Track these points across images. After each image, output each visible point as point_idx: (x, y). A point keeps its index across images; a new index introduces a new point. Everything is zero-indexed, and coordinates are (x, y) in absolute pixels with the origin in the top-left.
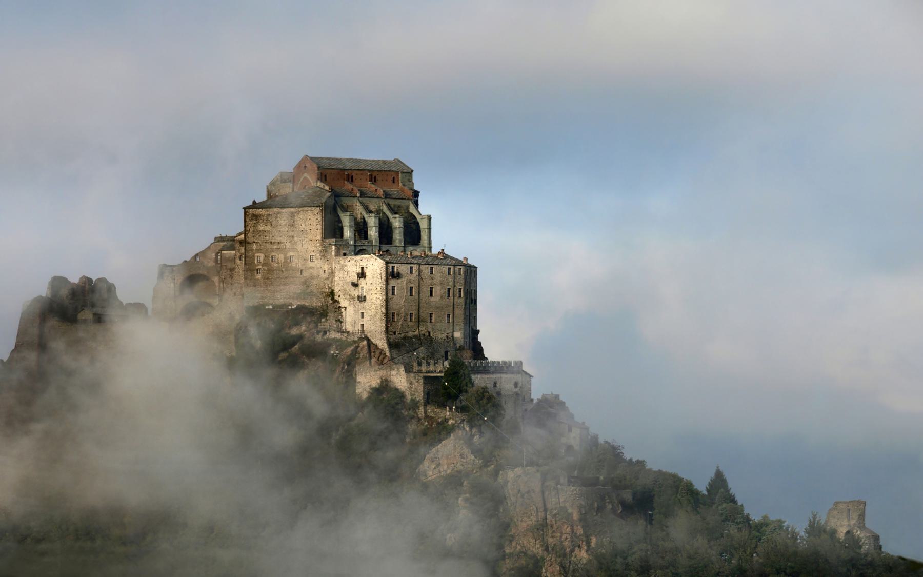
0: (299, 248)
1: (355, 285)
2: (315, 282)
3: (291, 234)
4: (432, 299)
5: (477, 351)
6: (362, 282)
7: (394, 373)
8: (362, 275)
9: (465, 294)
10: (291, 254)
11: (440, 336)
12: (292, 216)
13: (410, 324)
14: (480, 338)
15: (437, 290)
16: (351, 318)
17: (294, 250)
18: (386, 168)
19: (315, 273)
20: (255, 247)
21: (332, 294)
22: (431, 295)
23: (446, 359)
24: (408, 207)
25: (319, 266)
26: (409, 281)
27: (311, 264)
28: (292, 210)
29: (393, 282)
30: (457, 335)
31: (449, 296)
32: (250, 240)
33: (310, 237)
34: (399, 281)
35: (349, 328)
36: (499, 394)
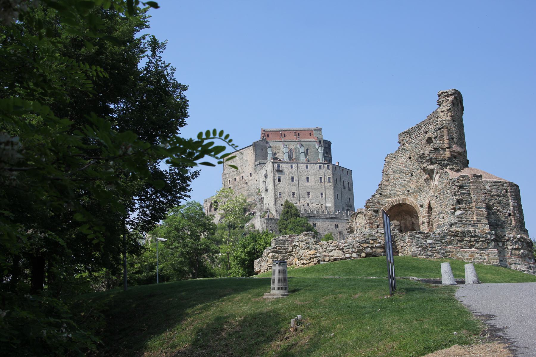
0: (245, 171)
2: (252, 188)
3: (241, 164)
4: (308, 184)
9: (334, 180)
10: (242, 175)
13: (294, 199)
17: (242, 172)
20: (227, 176)
22: (308, 181)
27: (251, 178)
30: (329, 205)
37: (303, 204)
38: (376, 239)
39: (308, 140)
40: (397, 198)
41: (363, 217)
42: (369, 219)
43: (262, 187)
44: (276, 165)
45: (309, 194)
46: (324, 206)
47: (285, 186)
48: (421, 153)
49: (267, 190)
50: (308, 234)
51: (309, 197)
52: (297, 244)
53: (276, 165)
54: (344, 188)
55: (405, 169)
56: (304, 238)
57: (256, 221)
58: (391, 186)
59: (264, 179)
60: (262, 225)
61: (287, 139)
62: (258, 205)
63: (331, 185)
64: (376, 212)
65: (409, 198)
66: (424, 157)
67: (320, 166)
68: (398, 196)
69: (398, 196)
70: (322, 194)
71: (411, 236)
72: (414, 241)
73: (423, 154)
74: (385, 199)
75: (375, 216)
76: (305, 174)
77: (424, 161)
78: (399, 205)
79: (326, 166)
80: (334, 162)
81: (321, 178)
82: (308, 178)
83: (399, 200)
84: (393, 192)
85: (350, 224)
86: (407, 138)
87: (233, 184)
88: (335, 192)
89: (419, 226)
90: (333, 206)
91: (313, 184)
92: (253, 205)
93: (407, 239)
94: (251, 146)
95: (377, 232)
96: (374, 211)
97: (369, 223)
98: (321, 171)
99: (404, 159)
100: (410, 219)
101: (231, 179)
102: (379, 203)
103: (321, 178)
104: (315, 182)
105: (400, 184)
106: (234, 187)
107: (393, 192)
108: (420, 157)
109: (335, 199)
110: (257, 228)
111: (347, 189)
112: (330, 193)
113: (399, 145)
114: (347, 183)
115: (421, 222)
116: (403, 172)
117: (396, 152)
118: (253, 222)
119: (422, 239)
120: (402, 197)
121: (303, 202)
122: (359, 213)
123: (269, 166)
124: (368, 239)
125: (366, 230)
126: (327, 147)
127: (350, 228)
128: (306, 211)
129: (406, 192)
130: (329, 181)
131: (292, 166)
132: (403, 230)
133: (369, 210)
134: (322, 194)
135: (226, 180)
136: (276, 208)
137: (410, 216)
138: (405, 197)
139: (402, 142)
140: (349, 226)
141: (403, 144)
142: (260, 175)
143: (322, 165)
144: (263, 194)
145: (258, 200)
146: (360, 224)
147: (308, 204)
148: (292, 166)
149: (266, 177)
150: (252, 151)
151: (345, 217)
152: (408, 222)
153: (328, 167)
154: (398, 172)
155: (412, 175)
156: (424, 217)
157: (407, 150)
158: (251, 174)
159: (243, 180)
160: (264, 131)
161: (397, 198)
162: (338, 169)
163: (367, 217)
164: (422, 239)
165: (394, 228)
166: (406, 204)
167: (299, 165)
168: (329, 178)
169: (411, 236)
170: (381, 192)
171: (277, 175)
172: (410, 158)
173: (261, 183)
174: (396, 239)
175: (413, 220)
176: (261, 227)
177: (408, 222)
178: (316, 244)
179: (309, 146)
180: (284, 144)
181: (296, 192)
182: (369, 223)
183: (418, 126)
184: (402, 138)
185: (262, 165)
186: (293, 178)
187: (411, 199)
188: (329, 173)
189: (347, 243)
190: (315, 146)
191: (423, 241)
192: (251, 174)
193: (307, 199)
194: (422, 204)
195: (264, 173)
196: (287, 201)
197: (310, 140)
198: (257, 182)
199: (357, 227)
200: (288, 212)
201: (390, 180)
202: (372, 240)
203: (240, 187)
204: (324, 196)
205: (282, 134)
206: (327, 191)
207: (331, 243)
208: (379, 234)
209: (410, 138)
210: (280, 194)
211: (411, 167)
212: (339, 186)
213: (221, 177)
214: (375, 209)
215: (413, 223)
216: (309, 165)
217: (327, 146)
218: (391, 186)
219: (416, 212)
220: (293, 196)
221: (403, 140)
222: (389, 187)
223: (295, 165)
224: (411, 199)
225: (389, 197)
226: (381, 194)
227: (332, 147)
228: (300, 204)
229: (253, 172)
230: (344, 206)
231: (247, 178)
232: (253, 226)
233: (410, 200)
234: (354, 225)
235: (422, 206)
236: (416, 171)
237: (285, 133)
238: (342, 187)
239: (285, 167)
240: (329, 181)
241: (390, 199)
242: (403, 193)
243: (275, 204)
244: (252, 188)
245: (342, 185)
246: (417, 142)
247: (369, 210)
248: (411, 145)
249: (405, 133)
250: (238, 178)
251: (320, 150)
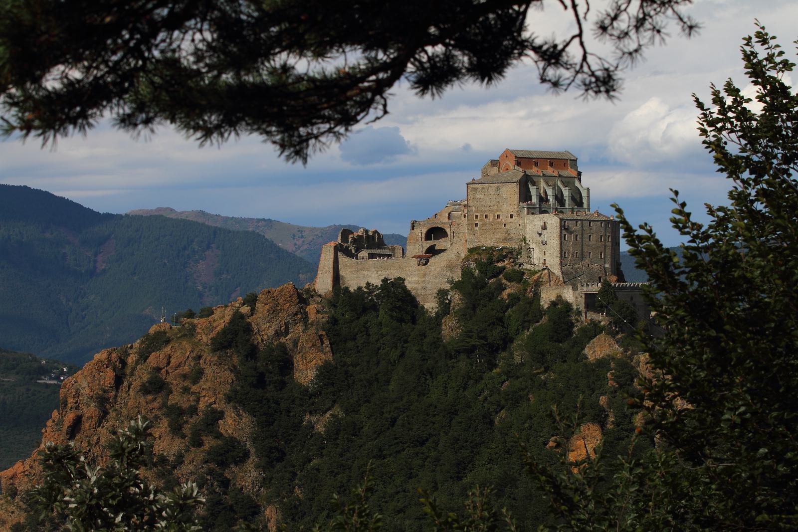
1: (540, 234)
2: (513, 232)
4: (590, 243)
5: (621, 278)
6: (544, 232)
7: (565, 291)
8: (544, 228)
12: (498, 188)
14: (622, 268)
16: (537, 255)
18: (559, 157)
19: (513, 226)
20: (474, 209)
21: (525, 239)
23: (600, 282)
24: (574, 183)
27: (511, 220)
29: (564, 232)
32: (470, 204)
34: (684, 39)
35: (536, 262)
36: (634, 305)
91: (594, 242)
158: (511, 216)
229: (515, 214)
250: (491, 216)
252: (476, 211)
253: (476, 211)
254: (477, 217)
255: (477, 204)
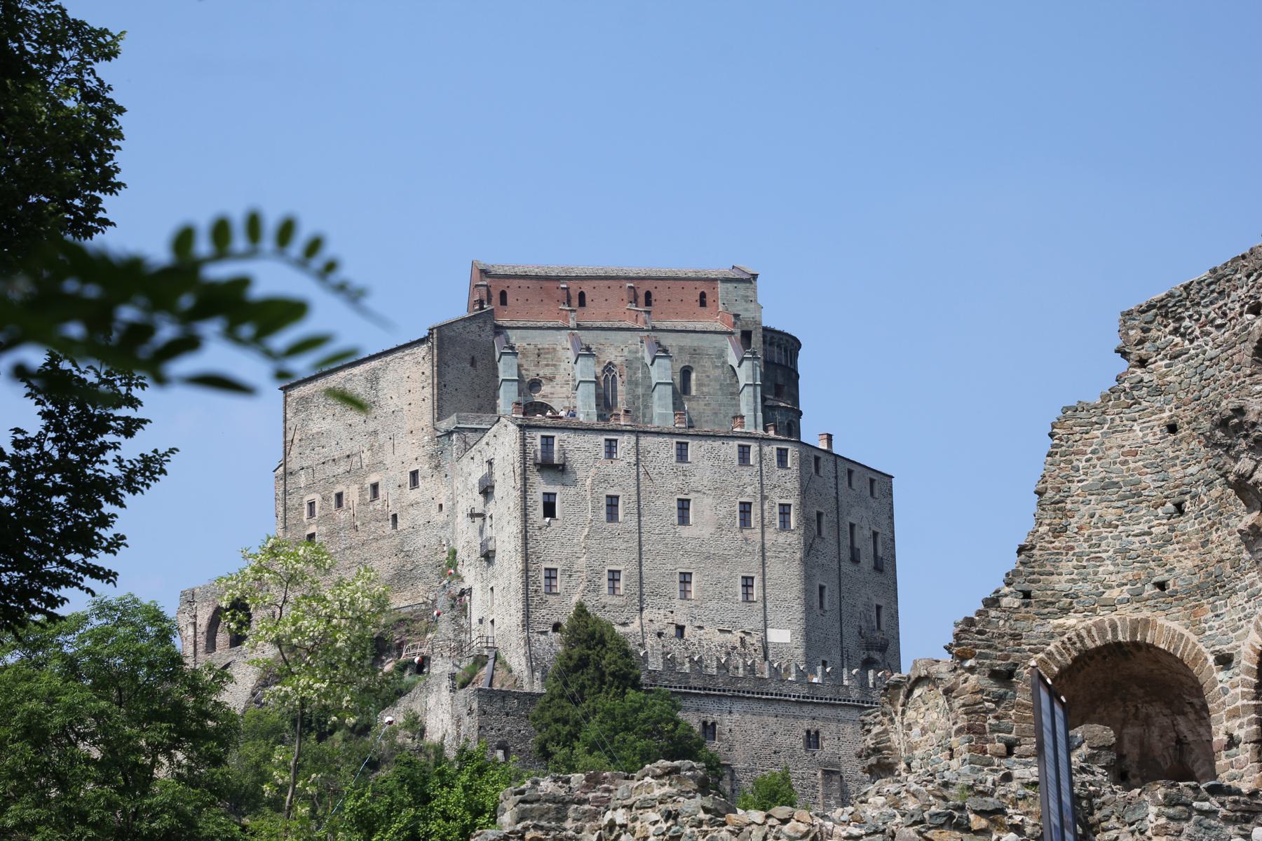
0: (389, 459)
2: (420, 541)
4: (685, 531)
9: (805, 519)
10: (373, 478)
11: (720, 638)
13: (616, 600)
15: (701, 508)
17: (374, 467)
20: (302, 480)
22: (684, 519)
25: (428, 495)
26: (606, 480)
27: (413, 495)
28: (374, 364)
30: (780, 636)
31: (745, 522)
33: (407, 427)
37: (656, 627)
38: (1001, 811)
39: (690, 326)
40: (1106, 616)
41: (942, 701)
42: (970, 709)
43: (465, 537)
44: (536, 438)
45: (685, 578)
46: (753, 640)
47: (574, 539)
48: (1227, 405)
49: (488, 556)
50: (676, 770)
51: (685, 594)
52: (620, 817)
53: (536, 438)
54: (855, 559)
55: (1147, 479)
56: (657, 793)
57: (432, 701)
58: (1079, 556)
59: (478, 503)
60: (458, 722)
61: (594, 314)
62: (445, 628)
63: (790, 541)
64: (1004, 677)
65: (1161, 620)
66: (1240, 426)
67: (744, 453)
68: (1112, 606)
69: (1112, 606)
70: (747, 583)
71: (1170, 802)
72: (1188, 827)
73: (1240, 411)
74: (1045, 617)
75: (999, 700)
76: (673, 483)
77: (1243, 444)
78: (1115, 649)
79: (771, 450)
80: (810, 432)
81: (745, 508)
82: (684, 506)
83: (1114, 627)
84: (1087, 587)
85: (876, 729)
86: (1162, 334)
87: (327, 518)
88: (808, 578)
89: (1210, 759)
90: (799, 641)
92: (421, 625)
93: (1152, 815)
94: (421, 341)
95: (1007, 778)
96: (995, 675)
97: (970, 729)
98: (748, 476)
99: (1143, 432)
100: (1166, 721)
101: (317, 498)
102: (1016, 637)
103: (745, 508)
104: (720, 527)
105: (1123, 551)
106: (332, 534)
107: (1087, 587)
108: (1223, 424)
109: (808, 609)
110: (433, 736)
111: (867, 562)
112: (785, 577)
113: (1123, 365)
114: (868, 533)
115: (1219, 737)
116: (1137, 494)
117: (1105, 398)
118: (416, 707)
119: (1226, 819)
120: (1128, 613)
121: (657, 617)
122: (919, 681)
123: (503, 444)
124: (961, 808)
125: (955, 763)
126: (779, 359)
127: (876, 750)
128: (670, 662)
129: (1149, 590)
130: (785, 524)
131: (611, 447)
132: (1133, 770)
133: (971, 670)
134: (747, 583)
135: (293, 501)
136: (528, 642)
137: (1169, 704)
138: (1146, 613)
139: (1136, 352)
140: (870, 742)
141: (1142, 363)
142: (458, 483)
143: (754, 448)
144: (470, 575)
145: (443, 602)
146: (924, 731)
147: (680, 629)
148: (611, 447)
149: (487, 491)
150: (427, 368)
151: (855, 695)
152: (1156, 732)
153: (782, 454)
154: (1112, 494)
155: (1179, 508)
156: (1234, 714)
157: (1158, 391)
158: (414, 474)
159: (378, 504)
160: (485, 273)
161: (1106, 616)
162: (827, 466)
163: (957, 703)
164: (1226, 819)
165: (1090, 758)
166: (1150, 647)
167: (646, 441)
168: (785, 510)
169: (1170, 802)
170: (1026, 586)
171: (540, 486)
172: (1172, 429)
173: (462, 521)
174: (1098, 815)
175: (1183, 726)
176: (451, 730)
177: (1156, 732)
178: (712, 823)
179: (695, 352)
180: (576, 342)
181: (626, 569)
182: (970, 729)
183: (1217, 276)
184: (1135, 334)
185: (468, 435)
186: (612, 502)
187: (1174, 625)
188: (786, 486)
189: (861, 822)
190: (721, 354)
191: (1231, 830)
192: (414, 474)
193: (677, 603)
194: (1225, 648)
195: (479, 472)
196: (581, 610)
197: (699, 326)
198: (442, 518)
199: (912, 748)
200: (583, 663)
201: (1073, 528)
202: (981, 813)
203: (362, 536)
204: (756, 592)
205: (570, 292)
206: (775, 569)
207: (784, 822)
208: (1014, 785)
209: (1175, 331)
210: (551, 574)
211: (1176, 473)
212: (828, 547)
213: (269, 487)
214: (1000, 665)
215: (1180, 741)
216: (693, 445)
217: (777, 355)
218: (1079, 556)
219: (1198, 690)
220: (613, 590)
221: (1141, 342)
222: (1067, 565)
223: (625, 443)
224: (1174, 625)
225: (1065, 611)
226: (1027, 595)
227: (805, 363)
228: (641, 629)
229: (424, 468)
230: (852, 642)
231: (394, 493)
232: (416, 726)
233: (1168, 628)
234: (896, 739)
235: (1225, 661)
236: (1201, 489)
237: (586, 287)
238: (846, 553)
239: (581, 450)
240: (785, 524)
241: (1071, 621)
242: (1137, 596)
243: (527, 623)
244: (420, 541)
245: (846, 542)
246: (1211, 353)
247: (971, 670)
248: (1179, 365)
249: (1150, 307)
250: (353, 495)
251: (746, 374)
252: (309, 487)
253: (309, 487)
254: (311, 504)
255: (311, 459)
